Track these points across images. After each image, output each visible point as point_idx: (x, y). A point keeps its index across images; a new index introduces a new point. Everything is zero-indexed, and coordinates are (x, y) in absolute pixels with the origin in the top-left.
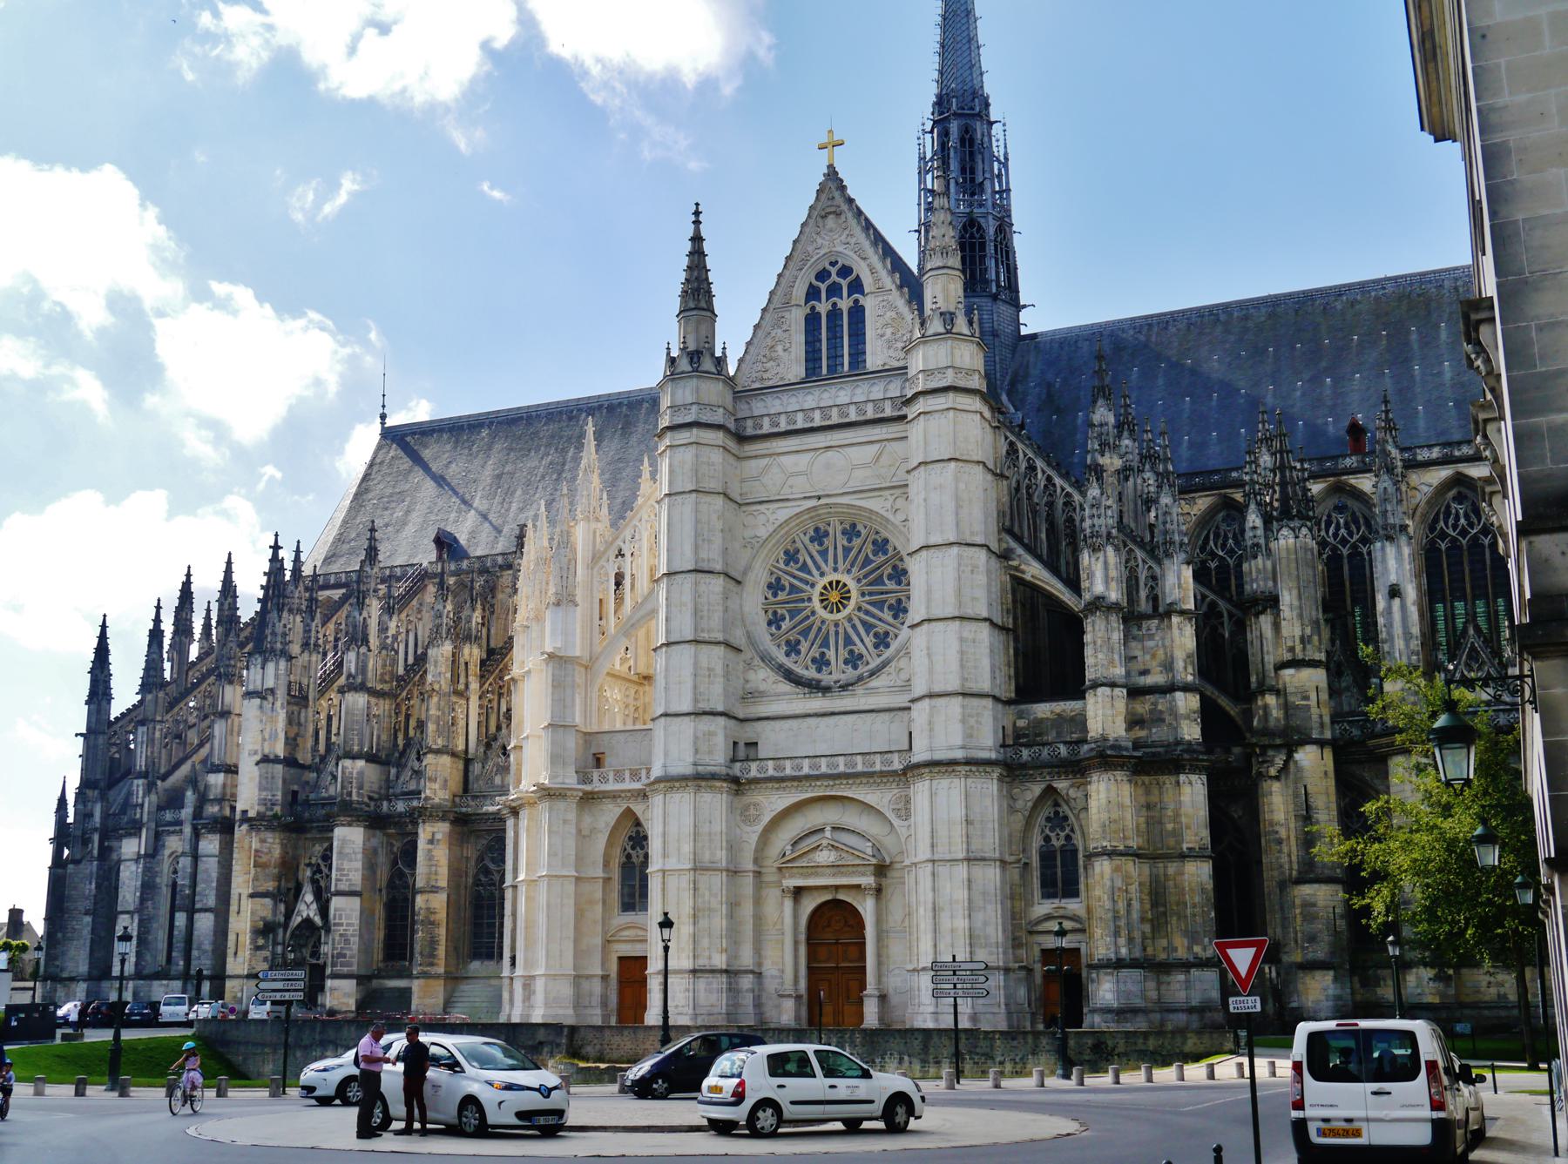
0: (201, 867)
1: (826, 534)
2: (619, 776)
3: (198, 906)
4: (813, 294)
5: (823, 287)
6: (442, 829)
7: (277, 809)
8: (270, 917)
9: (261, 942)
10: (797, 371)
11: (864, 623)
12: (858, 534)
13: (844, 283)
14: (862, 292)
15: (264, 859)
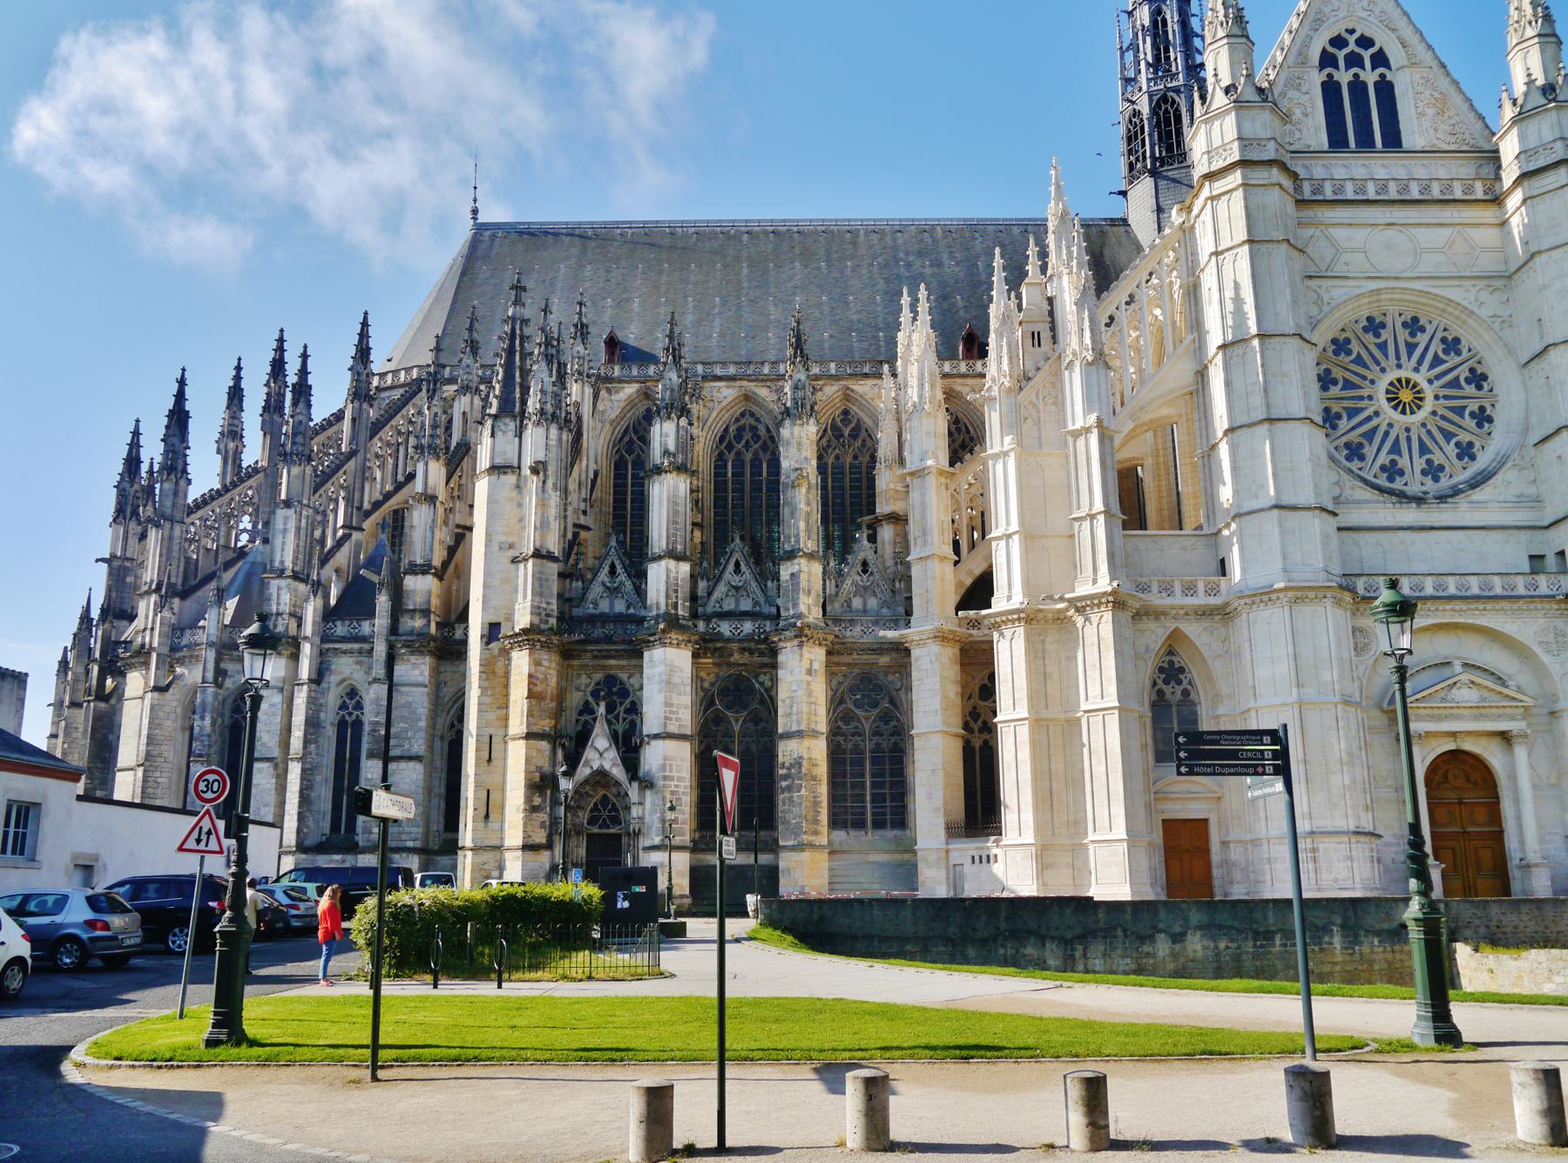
0: (398, 699)
1: (1383, 325)
2: (1167, 589)
3: (393, 753)
4: (1327, 60)
5: (1341, 55)
6: (816, 655)
7: (553, 621)
8: (547, 768)
9: (537, 801)
10: (1323, 140)
11: (1441, 429)
12: (1423, 330)
13: (1367, 55)
14: (1387, 65)
15: (538, 689)
